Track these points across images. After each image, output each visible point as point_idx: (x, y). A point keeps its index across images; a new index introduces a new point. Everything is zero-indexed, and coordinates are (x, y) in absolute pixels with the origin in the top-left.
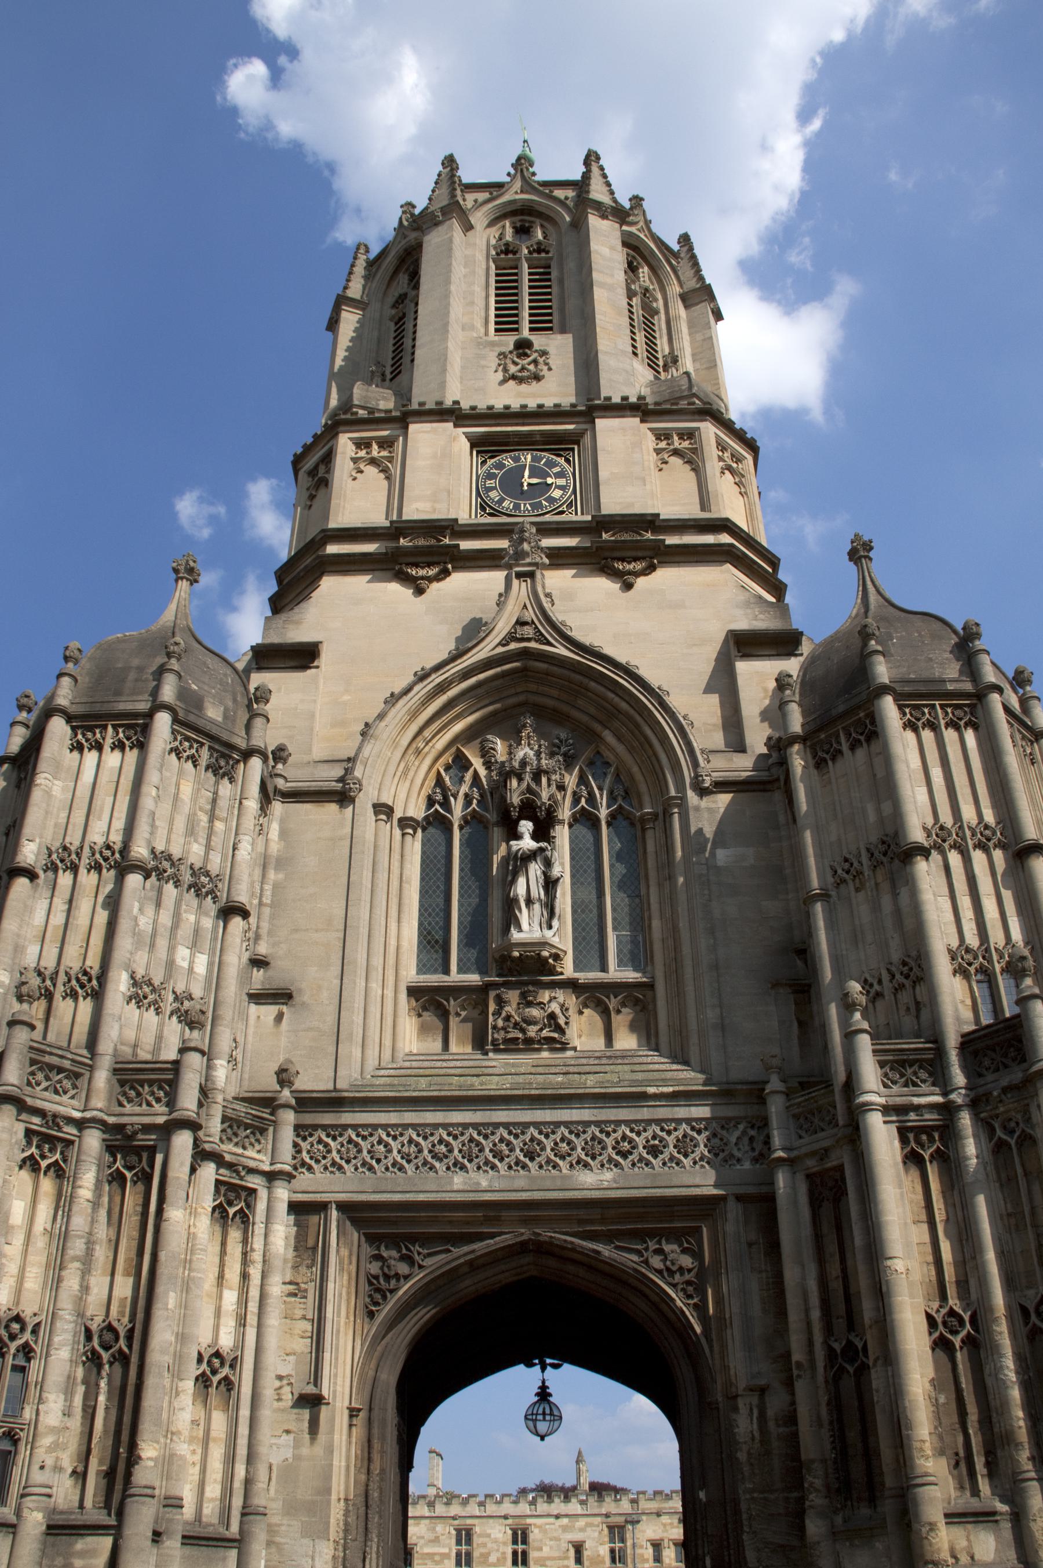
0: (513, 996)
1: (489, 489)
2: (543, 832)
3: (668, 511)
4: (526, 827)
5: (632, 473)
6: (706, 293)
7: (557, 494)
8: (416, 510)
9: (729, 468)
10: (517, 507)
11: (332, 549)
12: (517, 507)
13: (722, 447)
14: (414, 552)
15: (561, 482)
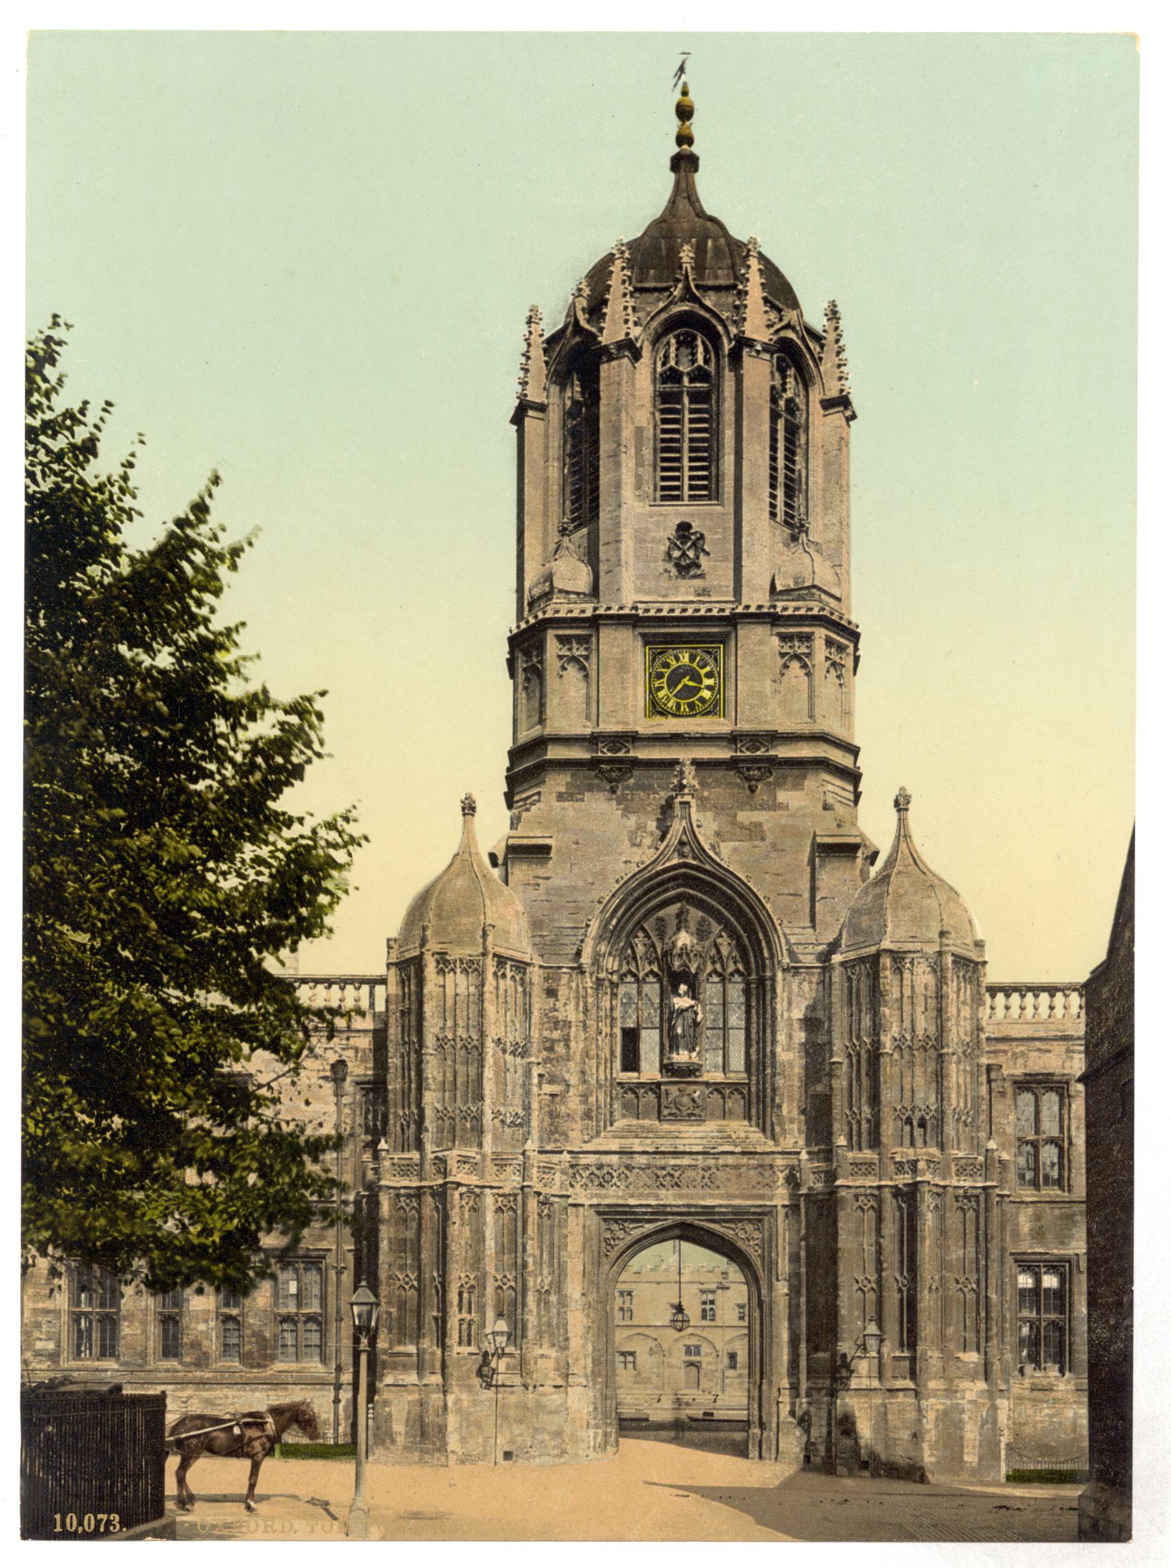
0: (674, 1091)
1: (660, 689)
2: (694, 993)
3: (784, 726)
4: (683, 988)
5: (761, 689)
6: (843, 402)
7: (706, 694)
8: (609, 726)
9: (834, 664)
10: (678, 706)
11: (555, 753)
12: (678, 706)
13: (829, 643)
14: (611, 763)
15: (710, 682)
